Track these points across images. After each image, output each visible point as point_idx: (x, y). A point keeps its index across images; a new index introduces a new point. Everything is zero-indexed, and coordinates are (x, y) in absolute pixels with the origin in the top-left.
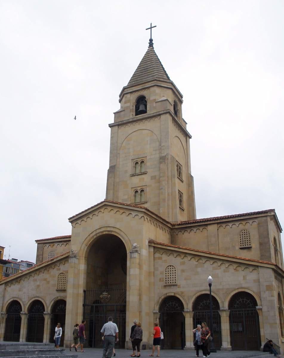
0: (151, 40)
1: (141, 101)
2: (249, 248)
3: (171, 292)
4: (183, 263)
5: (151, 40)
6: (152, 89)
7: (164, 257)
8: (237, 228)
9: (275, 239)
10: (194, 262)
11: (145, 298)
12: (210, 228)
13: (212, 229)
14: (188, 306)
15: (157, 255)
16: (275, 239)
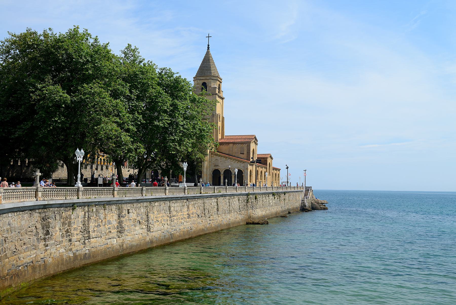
0: (208, 45)
1: (204, 84)
2: (243, 154)
3: (217, 168)
4: (221, 159)
5: (208, 45)
6: (210, 80)
7: (215, 156)
8: (240, 146)
9: (253, 150)
10: (224, 159)
11: (208, 170)
12: (230, 145)
13: (231, 145)
14: (222, 173)
15: (212, 155)
16: (253, 150)
